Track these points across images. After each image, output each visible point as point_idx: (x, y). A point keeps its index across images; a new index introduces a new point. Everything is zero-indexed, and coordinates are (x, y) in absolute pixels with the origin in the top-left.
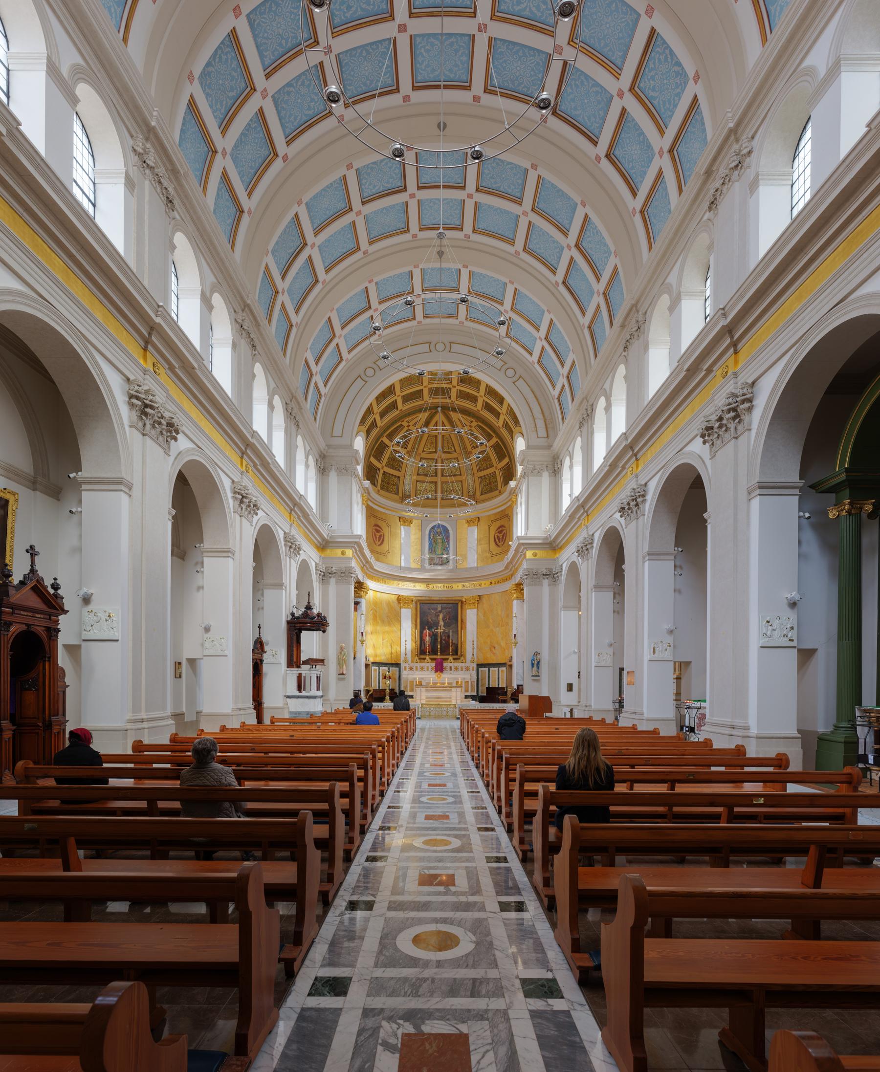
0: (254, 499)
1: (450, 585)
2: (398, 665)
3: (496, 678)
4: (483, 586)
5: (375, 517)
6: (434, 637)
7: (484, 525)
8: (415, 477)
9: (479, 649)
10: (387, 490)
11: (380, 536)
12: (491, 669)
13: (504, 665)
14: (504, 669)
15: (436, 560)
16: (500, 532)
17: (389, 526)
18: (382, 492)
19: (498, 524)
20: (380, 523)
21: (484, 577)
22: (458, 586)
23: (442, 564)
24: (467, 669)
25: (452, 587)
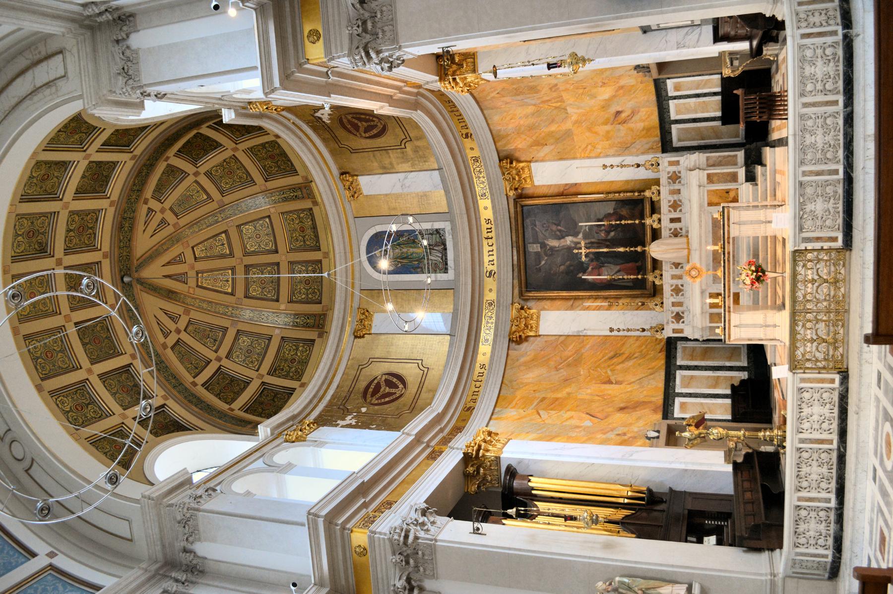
0: (413, 515)
1: (484, 226)
2: (671, 345)
3: (697, 102)
4: (476, 153)
5: (347, 399)
6: (599, 260)
7: (355, 162)
8: (325, 275)
9: (625, 148)
10: (305, 363)
11: (389, 384)
12: (673, 116)
13: (659, 88)
14: (670, 83)
15: (436, 257)
16: (357, 128)
17: (371, 361)
18: (304, 380)
19: (341, 133)
20: (362, 385)
21: (457, 155)
22: (486, 208)
23: (444, 244)
24: (675, 178)
25: (488, 221)
